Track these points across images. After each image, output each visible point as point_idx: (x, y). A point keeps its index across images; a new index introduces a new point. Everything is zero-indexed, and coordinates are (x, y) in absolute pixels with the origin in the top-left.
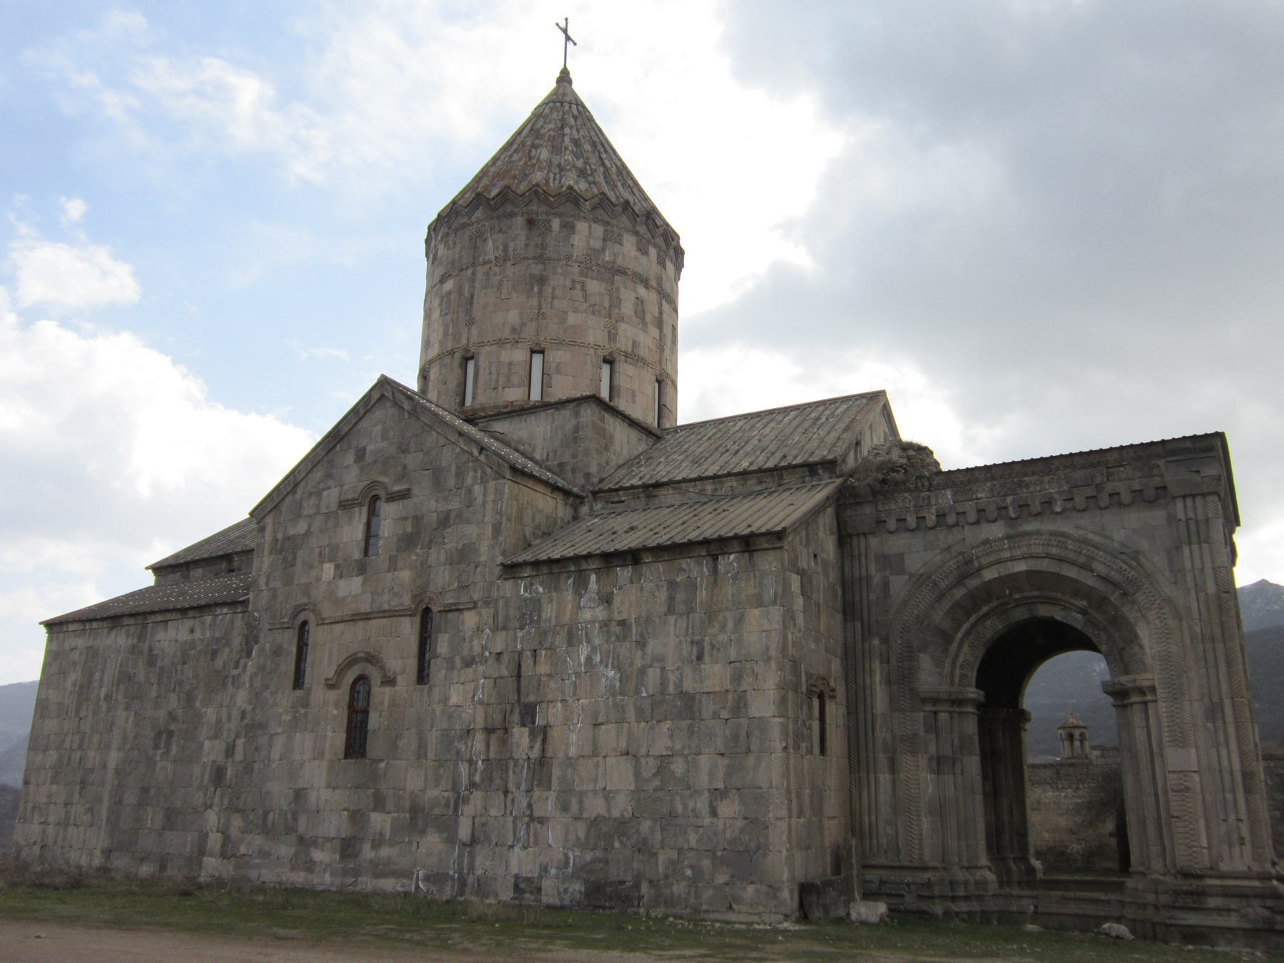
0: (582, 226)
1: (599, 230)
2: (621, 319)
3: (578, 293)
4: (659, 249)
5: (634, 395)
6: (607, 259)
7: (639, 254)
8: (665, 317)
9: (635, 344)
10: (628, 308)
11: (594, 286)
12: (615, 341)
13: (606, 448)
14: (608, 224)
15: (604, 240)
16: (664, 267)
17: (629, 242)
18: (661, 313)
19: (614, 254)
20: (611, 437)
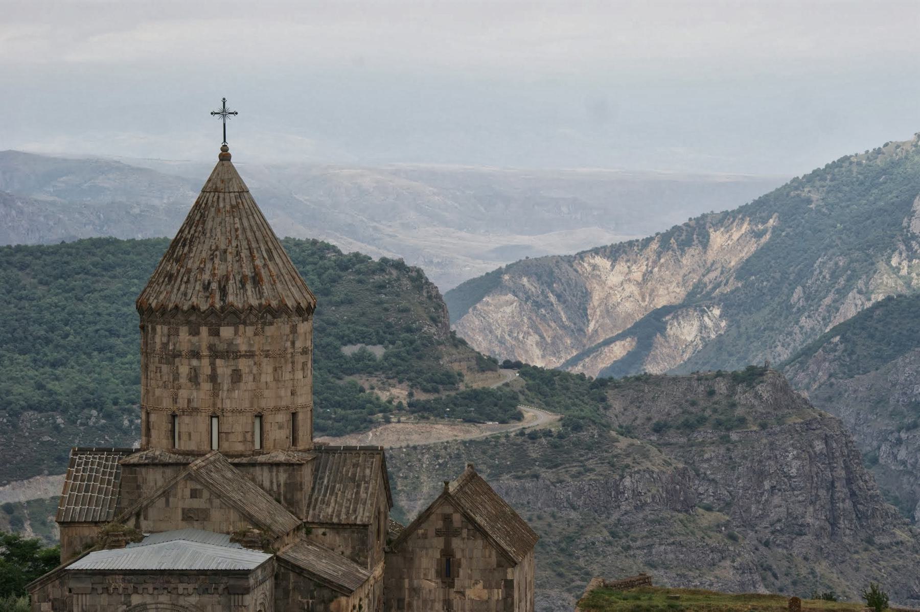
0: (158, 328)
1: (165, 328)
2: (179, 388)
3: (159, 375)
4: (209, 325)
5: (190, 434)
6: (171, 348)
7: (191, 337)
8: (220, 371)
9: (189, 401)
10: (183, 380)
11: (165, 368)
12: (176, 402)
13: (138, 487)
14: (169, 323)
15: (169, 336)
16: (217, 333)
17: (184, 333)
18: (214, 369)
19: (174, 345)
20: (145, 481)
